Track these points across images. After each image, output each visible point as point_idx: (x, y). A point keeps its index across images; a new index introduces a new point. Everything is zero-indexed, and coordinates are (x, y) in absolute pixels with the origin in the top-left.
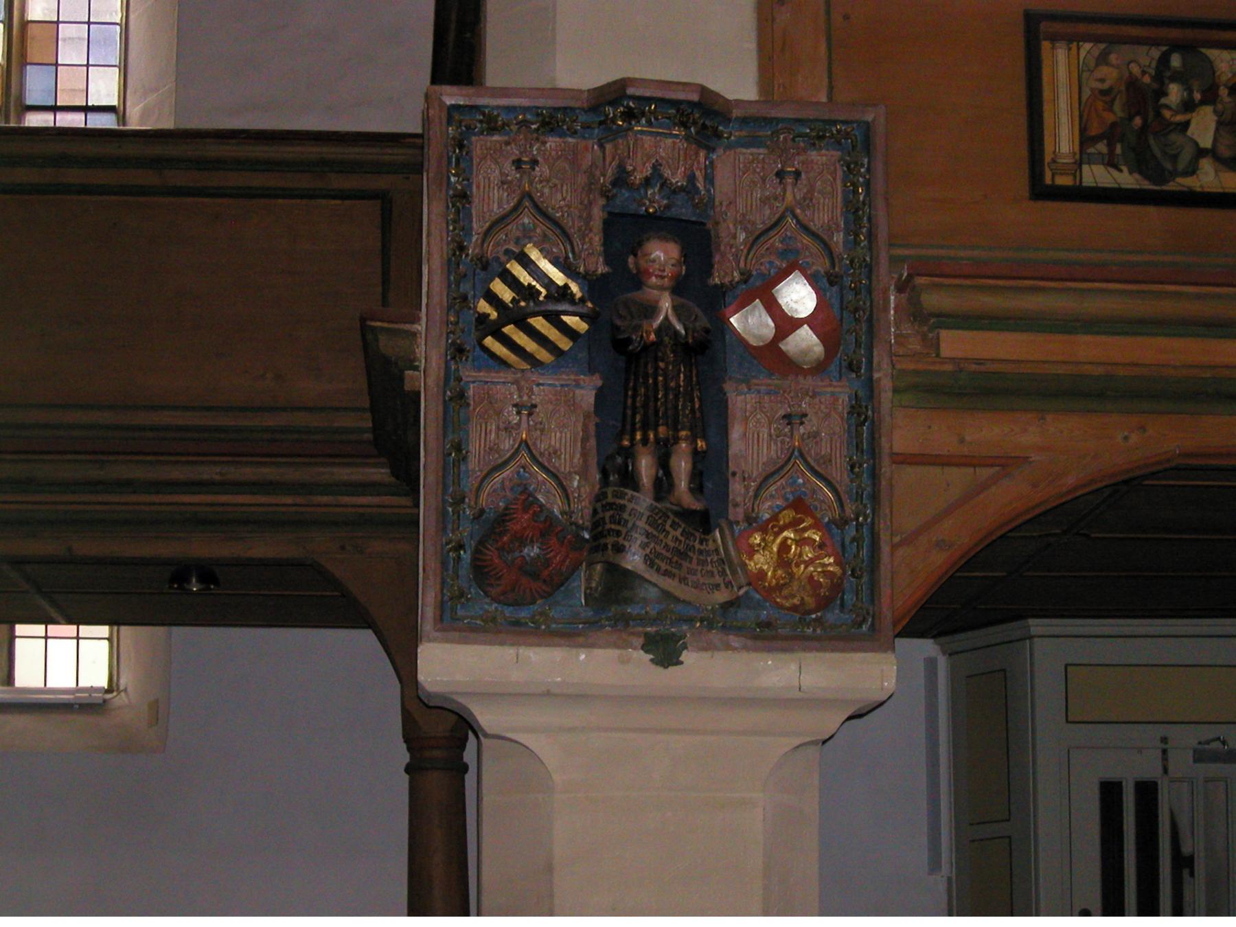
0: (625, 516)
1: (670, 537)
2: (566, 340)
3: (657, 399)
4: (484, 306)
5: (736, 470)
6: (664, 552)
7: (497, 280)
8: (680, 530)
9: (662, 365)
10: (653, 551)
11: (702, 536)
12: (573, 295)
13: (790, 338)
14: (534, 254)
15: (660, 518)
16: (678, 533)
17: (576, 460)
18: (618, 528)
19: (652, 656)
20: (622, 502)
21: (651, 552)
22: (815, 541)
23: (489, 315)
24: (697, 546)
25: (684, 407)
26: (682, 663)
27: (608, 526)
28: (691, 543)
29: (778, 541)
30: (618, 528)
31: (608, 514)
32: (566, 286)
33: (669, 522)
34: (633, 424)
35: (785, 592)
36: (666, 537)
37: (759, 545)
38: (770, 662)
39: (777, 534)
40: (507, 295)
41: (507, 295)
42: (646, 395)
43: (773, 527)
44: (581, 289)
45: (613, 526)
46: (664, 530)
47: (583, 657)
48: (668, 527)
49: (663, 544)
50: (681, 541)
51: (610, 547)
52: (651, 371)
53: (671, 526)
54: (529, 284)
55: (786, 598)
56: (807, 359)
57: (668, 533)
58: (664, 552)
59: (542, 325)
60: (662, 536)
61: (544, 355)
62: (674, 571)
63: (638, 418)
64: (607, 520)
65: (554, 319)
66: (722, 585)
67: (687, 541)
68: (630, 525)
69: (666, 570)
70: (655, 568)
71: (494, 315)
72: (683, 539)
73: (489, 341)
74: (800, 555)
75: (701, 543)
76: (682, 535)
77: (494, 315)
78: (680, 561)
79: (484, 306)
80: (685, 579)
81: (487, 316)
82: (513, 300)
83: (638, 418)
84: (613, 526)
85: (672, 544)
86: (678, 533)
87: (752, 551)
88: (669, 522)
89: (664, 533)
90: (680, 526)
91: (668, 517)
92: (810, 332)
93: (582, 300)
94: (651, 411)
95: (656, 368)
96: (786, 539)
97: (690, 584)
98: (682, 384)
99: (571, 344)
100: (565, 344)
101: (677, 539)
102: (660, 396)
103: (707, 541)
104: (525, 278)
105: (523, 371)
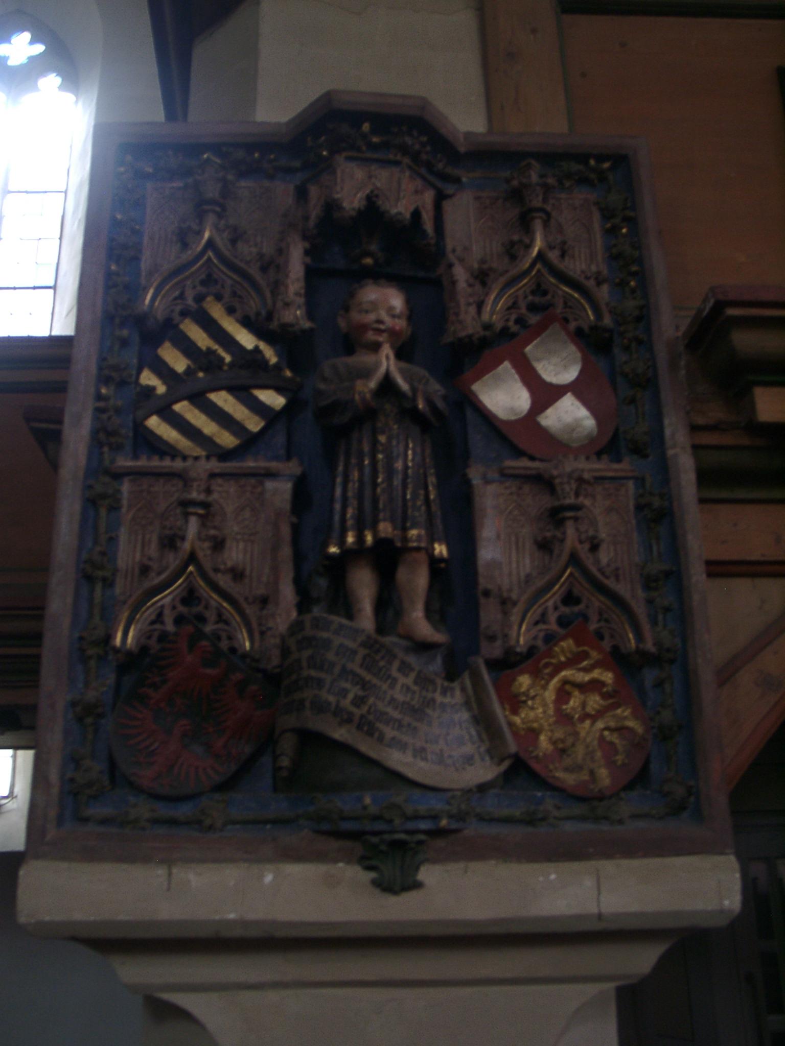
0: (331, 656)
1: (398, 687)
2: (256, 418)
3: (375, 485)
4: (148, 378)
5: (489, 586)
6: (389, 710)
7: (167, 344)
8: (412, 676)
9: (382, 439)
10: (372, 710)
11: (446, 684)
12: (265, 362)
13: (549, 411)
14: (217, 311)
15: (383, 658)
16: (409, 680)
17: (264, 579)
18: (322, 675)
19: (373, 875)
20: (325, 635)
21: (369, 712)
22: (603, 684)
23: (153, 389)
24: (439, 698)
25: (415, 496)
26: (418, 885)
27: (305, 673)
28: (430, 695)
29: (555, 680)
30: (322, 675)
31: (306, 653)
32: (257, 350)
33: (396, 664)
34: (343, 520)
35: (567, 761)
36: (392, 686)
37: (526, 694)
38: (553, 877)
39: (552, 676)
40: (180, 364)
41: (180, 364)
42: (361, 481)
43: (547, 665)
44: (278, 354)
45: (313, 673)
46: (389, 677)
47: (269, 878)
48: (395, 673)
49: (388, 698)
50: (414, 692)
51: (307, 704)
52: (366, 448)
53: (399, 670)
54: (209, 349)
55: (567, 770)
56: (575, 435)
57: (395, 680)
58: (389, 710)
59: (226, 401)
60: (385, 687)
61: (227, 440)
62: (405, 738)
63: (350, 512)
64: (304, 664)
65: (241, 392)
66: (477, 757)
67: (424, 693)
68: (337, 670)
69: (393, 738)
70: (376, 735)
71: (161, 389)
72: (416, 688)
73: (153, 422)
74: (584, 705)
75: (444, 692)
76: (416, 683)
77: (161, 389)
78: (415, 724)
79: (148, 378)
80: (423, 749)
81: (152, 389)
82: (189, 371)
83: (350, 512)
84: (313, 673)
85: (400, 697)
86: (409, 680)
87: (515, 703)
88: (396, 664)
89: (389, 681)
90: (412, 669)
91: (394, 656)
92: (578, 403)
93: (277, 367)
94: (367, 504)
95: (375, 443)
96: (565, 682)
97: (429, 757)
98: (410, 464)
99: (262, 424)
100: (254, 424)
101: (408, 688)
102: (380, 480)
103: (452, 689)
104: (201, 338)
105: (196, 458)
